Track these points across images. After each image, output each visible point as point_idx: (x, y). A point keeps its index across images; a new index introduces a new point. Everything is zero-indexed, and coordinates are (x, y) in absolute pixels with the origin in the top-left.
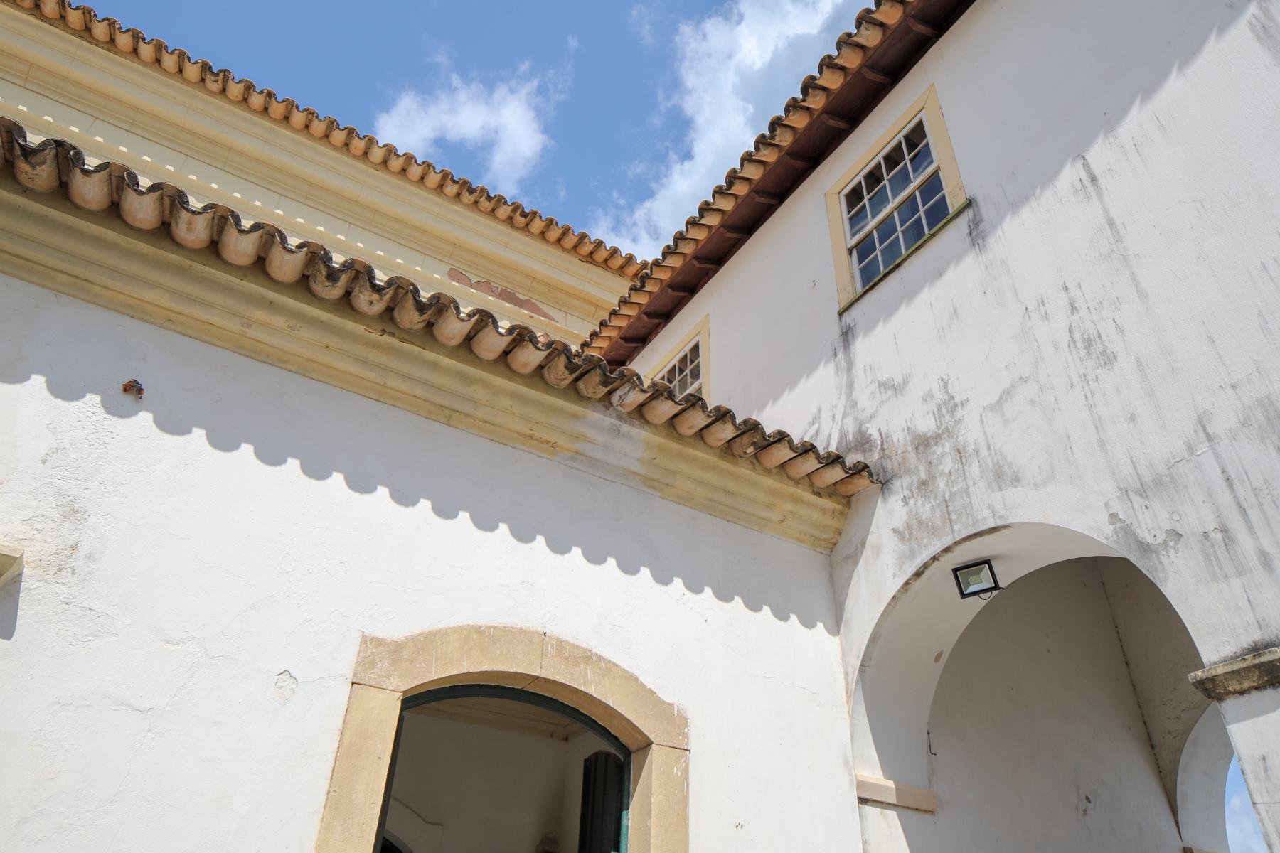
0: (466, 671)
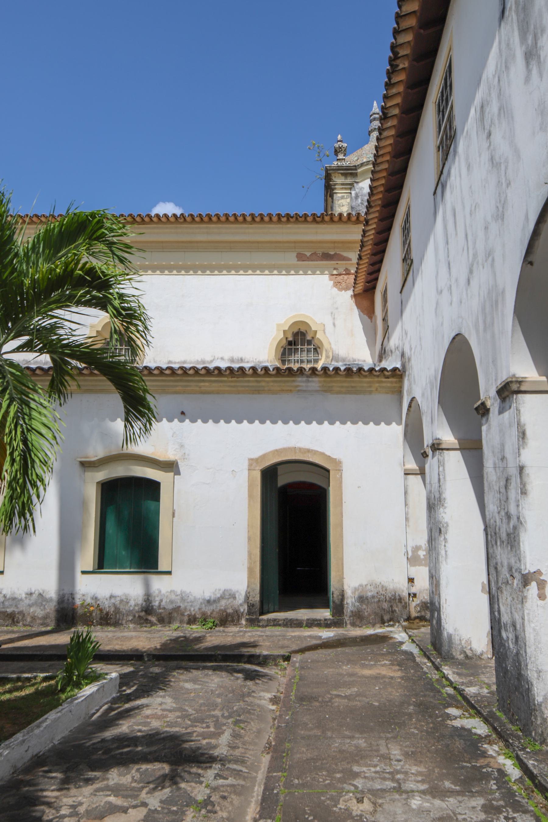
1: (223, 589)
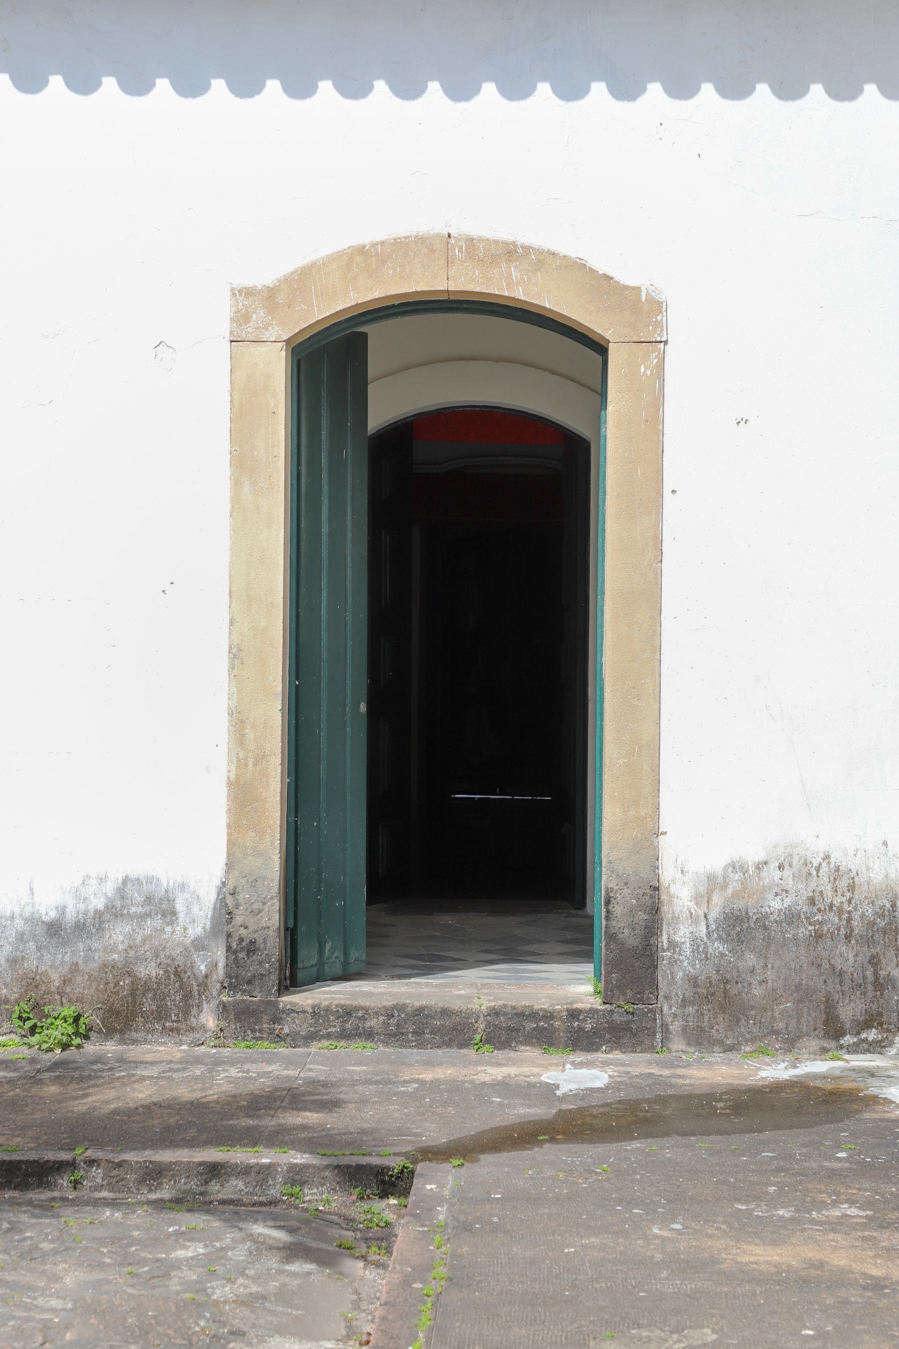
0: (354, 303)
1: (116, 877)
